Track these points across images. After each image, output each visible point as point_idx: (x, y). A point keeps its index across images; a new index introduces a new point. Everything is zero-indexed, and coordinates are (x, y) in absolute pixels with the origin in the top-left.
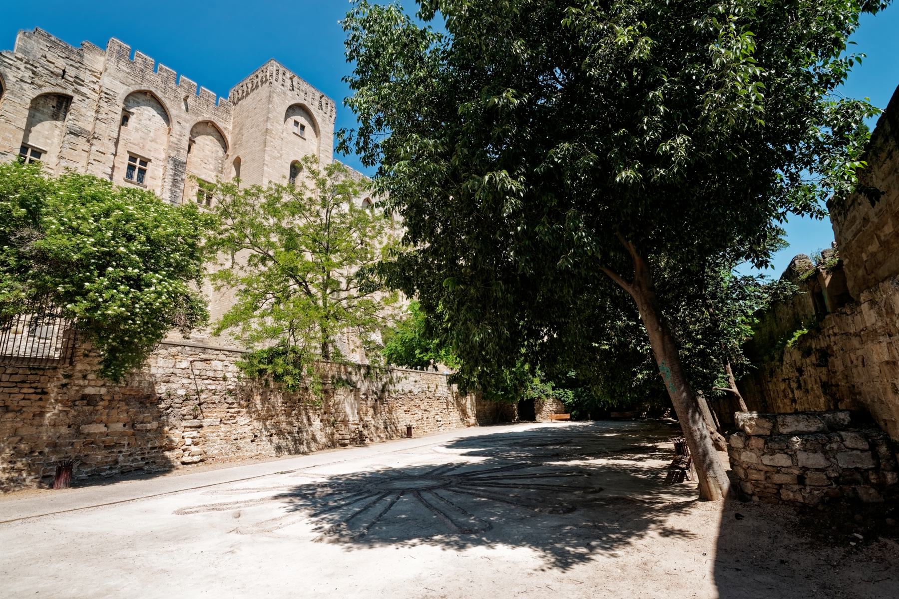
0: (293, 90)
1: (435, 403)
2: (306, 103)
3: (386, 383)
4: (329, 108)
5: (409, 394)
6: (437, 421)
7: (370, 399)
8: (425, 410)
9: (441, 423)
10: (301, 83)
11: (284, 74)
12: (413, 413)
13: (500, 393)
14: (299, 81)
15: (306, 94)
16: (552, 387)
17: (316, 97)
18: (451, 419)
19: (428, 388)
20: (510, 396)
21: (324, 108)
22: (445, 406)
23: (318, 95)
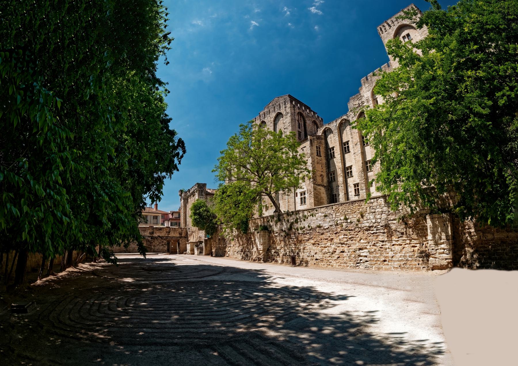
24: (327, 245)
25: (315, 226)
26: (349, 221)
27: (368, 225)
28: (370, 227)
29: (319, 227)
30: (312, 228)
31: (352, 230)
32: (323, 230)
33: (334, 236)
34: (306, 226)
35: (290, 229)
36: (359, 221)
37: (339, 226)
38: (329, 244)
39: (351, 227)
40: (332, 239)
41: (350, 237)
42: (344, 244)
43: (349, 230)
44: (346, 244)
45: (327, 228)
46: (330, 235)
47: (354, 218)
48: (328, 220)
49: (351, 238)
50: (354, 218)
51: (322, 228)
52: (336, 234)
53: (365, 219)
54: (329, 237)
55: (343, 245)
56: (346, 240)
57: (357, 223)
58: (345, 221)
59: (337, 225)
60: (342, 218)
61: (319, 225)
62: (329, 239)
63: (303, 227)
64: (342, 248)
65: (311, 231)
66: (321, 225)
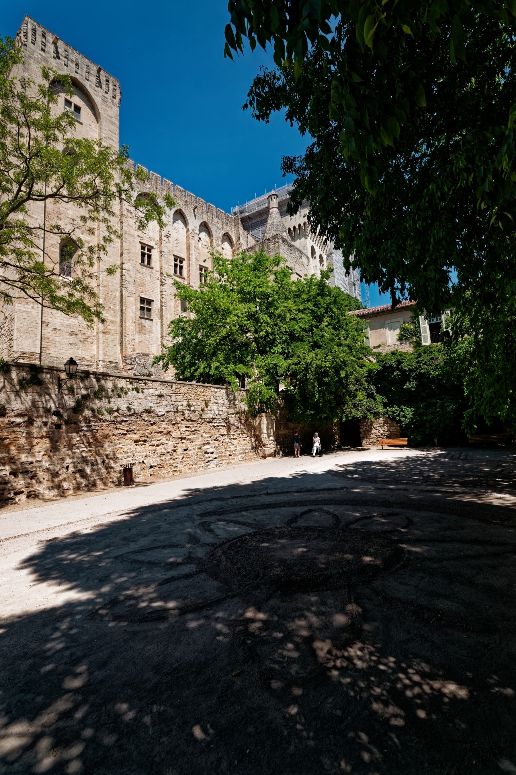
0: (59, 58)
1: (205, 427)
2: (78, 77)
3: (85, 397)
4: (111, 87)
5: (145, 416)
6: (206, 453)
7: (38, 422)
8: (182, 439)
9: (214, 455)
10: (70, 51)
11: (44, 36)
12: (155, 443)
13: (308, 412)
14: (67, 48)
15: (77, 65)
16: (384, 403)
17: (92, 72)
18: (233, 448)
19: (189, 405)
20: (324, 416)
21: (104, 86)
22: (223, 431)
23: (94, 69)
24: (161, 442)
25: (142, 410)
26: (192, 408)
27: (211, 416)
28: (213, 419)
29: (148, 411)
30: (134, 413)
31: (195, 421)
32: (154, 417)
33: (171, 428)
34: (124, 407)
35: (78, 408)
36: (203, 410)
37: (179, 414)
38: (163, 440)
39: (193, 416)
40: (169, 432)
41: (193, 429)
42: (185, 439)
43: (192, 421)
44: (188, 439)
45: (162, 415)
46: (166, 426)
47: (198, 405)
48: (164, 403)
49: (195, 430)
50: (198, 405)
51: (153, 415)
52: (174, 424)
53: (209, 409)
54: (165, 428)
55: (183, 441)
56: (188, 433)
57: (202, 412)
58: (187, 408)
59: (177, 412)
60: (185, 403)
61: (148, 408)
62: (165, 431)
63: (115, 408)
64: (184, 445)
65: (132, 418)
66: (153, 409)
